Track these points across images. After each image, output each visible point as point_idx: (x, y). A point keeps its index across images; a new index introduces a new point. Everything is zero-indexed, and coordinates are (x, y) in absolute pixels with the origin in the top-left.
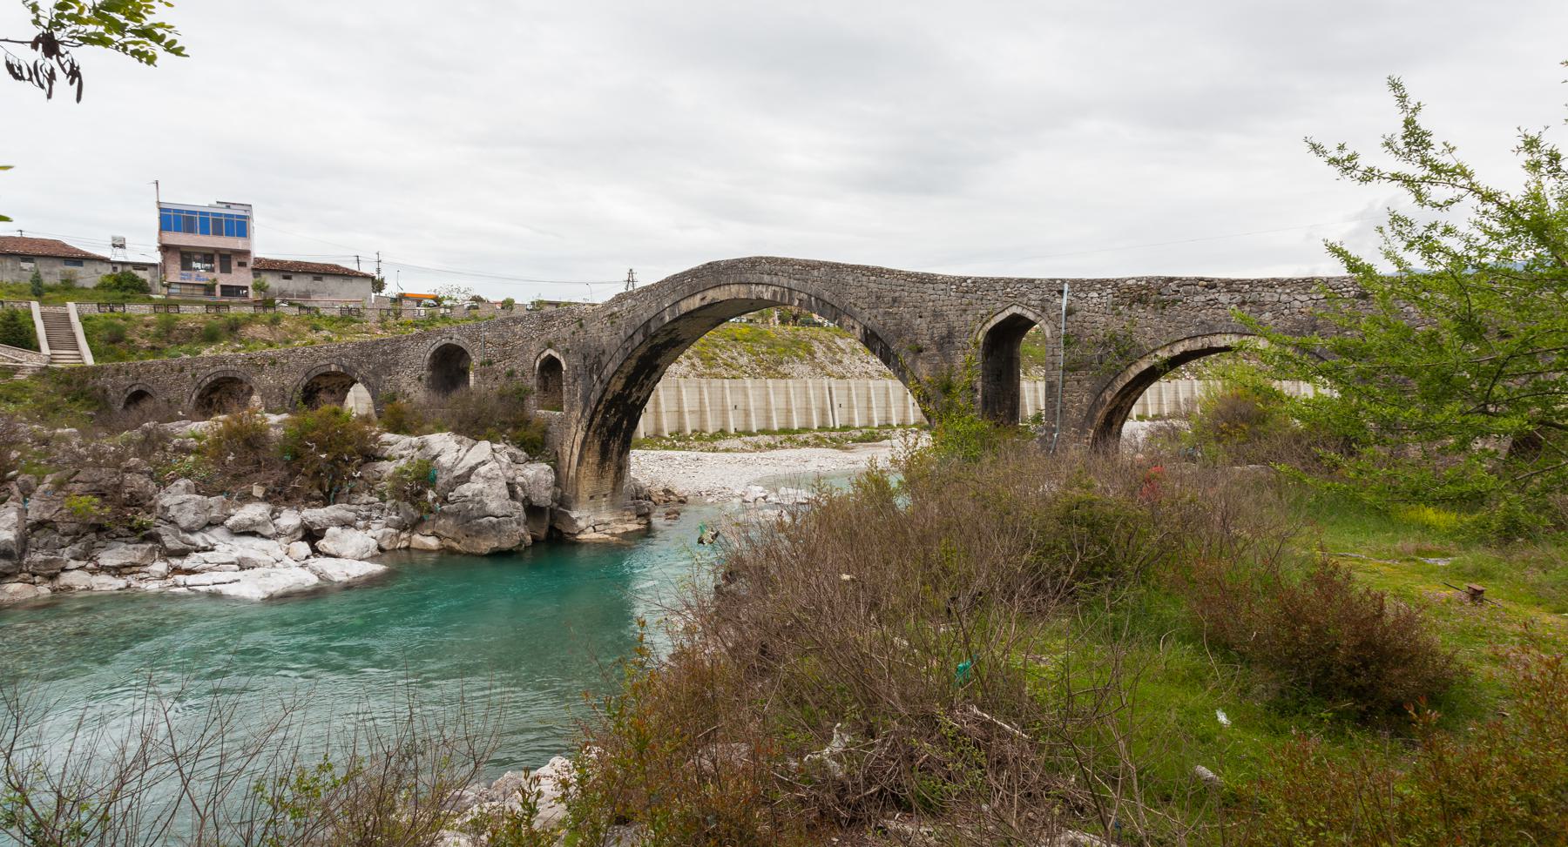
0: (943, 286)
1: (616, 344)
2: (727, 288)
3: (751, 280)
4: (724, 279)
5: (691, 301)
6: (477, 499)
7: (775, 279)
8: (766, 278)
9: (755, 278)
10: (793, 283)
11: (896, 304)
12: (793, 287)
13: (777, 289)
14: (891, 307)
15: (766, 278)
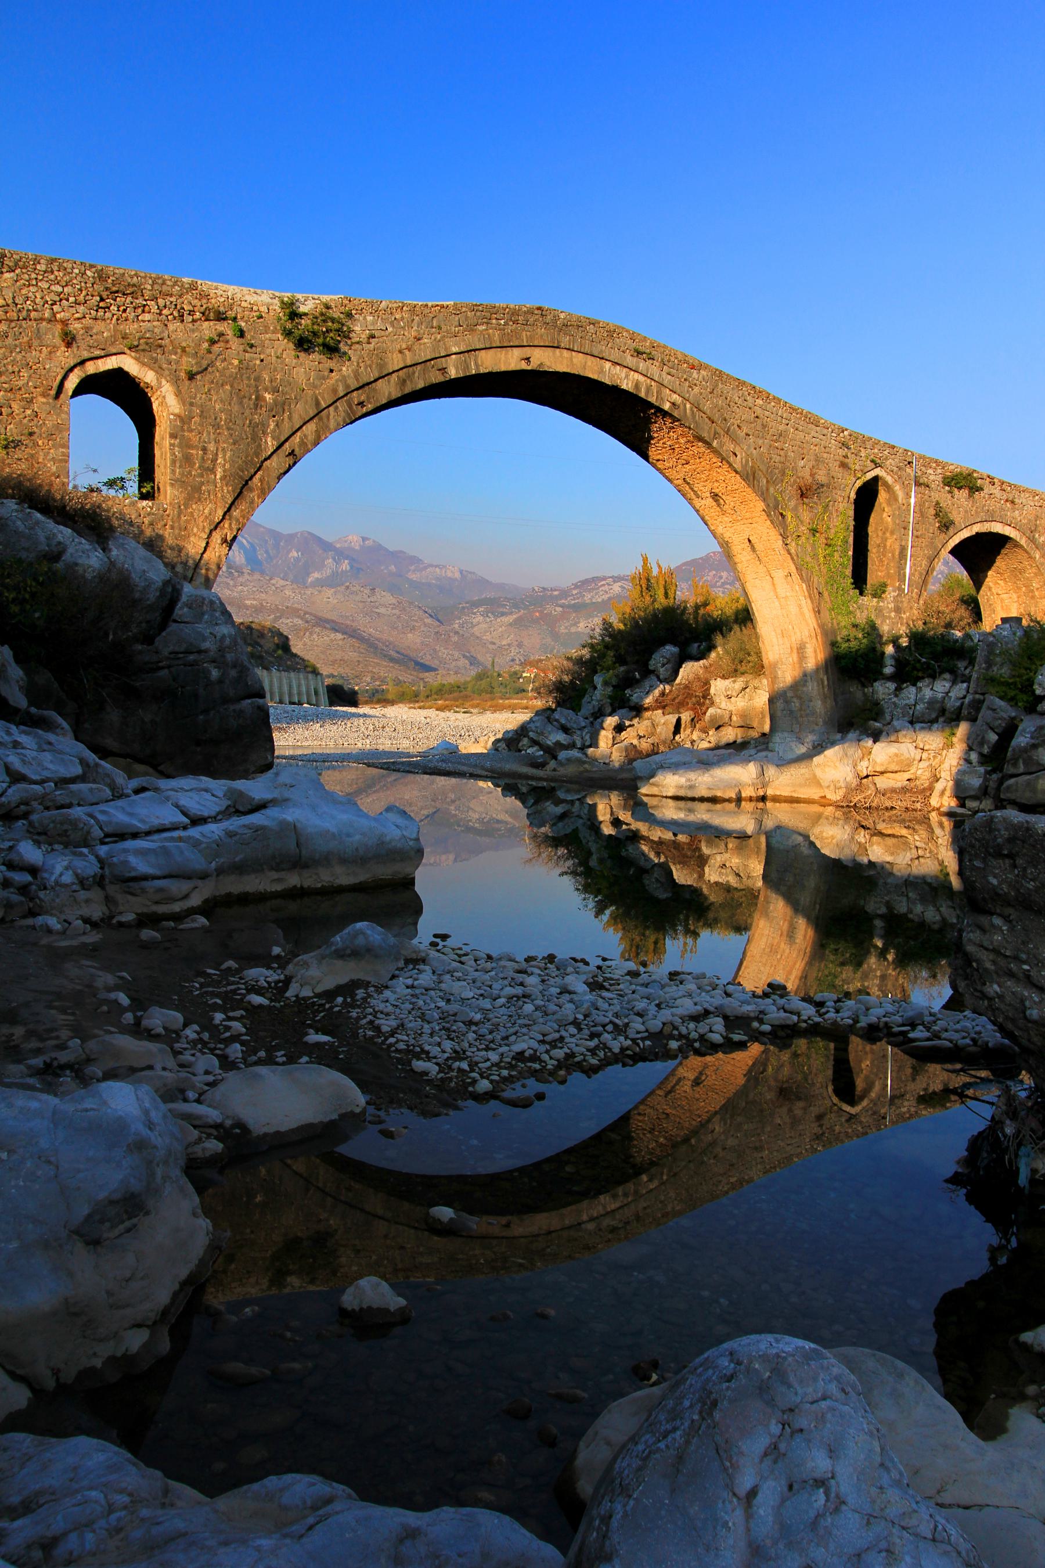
0: (825, 431)
1: (335, 391)
2: (565, 353)
3: (606, 355)
4: (565, 341)
5: (501, 354)
6: (230, 657)
7: (642, 366)
8: (630, 360)
9: (615, 355)
10: (667, 379)
11: (782, 439)
12: (665, 383)
13: (641, 378)
14: (776, 441)
15: (630, 360)
